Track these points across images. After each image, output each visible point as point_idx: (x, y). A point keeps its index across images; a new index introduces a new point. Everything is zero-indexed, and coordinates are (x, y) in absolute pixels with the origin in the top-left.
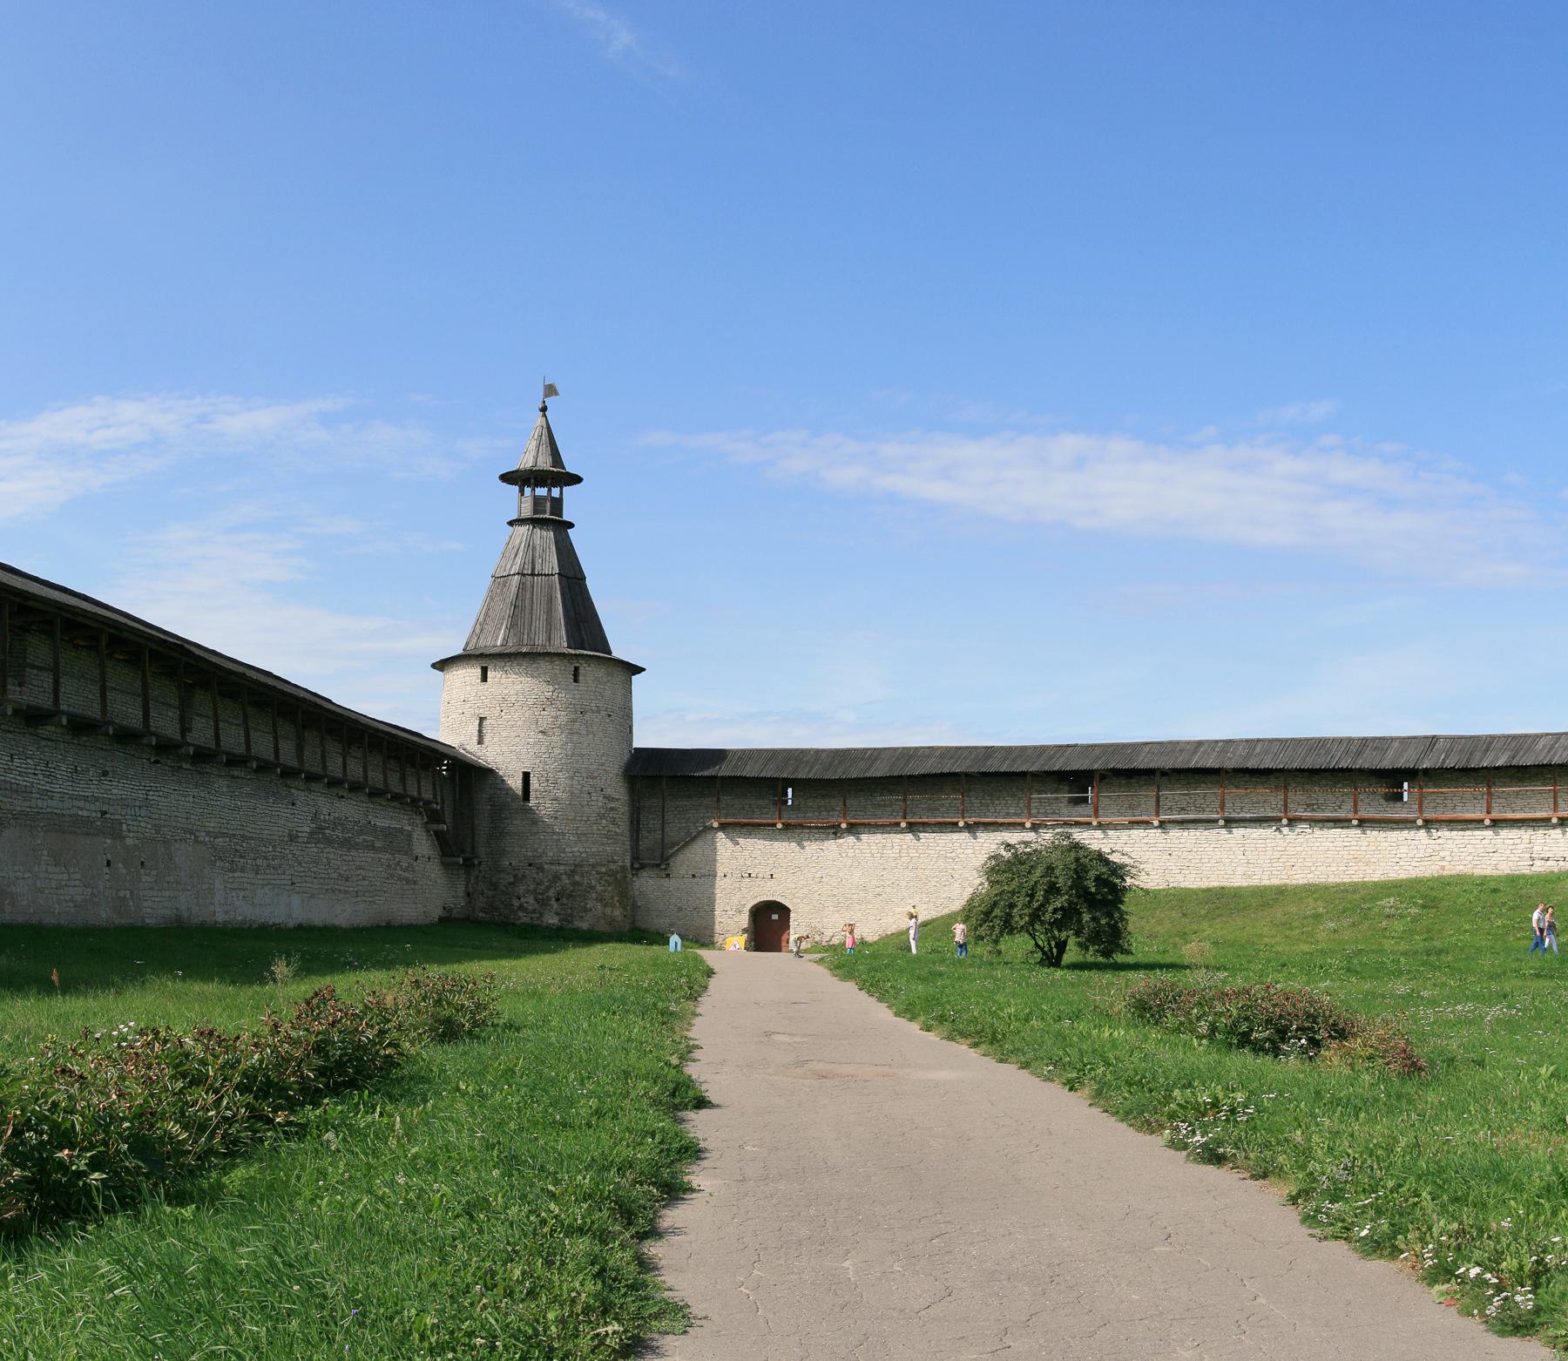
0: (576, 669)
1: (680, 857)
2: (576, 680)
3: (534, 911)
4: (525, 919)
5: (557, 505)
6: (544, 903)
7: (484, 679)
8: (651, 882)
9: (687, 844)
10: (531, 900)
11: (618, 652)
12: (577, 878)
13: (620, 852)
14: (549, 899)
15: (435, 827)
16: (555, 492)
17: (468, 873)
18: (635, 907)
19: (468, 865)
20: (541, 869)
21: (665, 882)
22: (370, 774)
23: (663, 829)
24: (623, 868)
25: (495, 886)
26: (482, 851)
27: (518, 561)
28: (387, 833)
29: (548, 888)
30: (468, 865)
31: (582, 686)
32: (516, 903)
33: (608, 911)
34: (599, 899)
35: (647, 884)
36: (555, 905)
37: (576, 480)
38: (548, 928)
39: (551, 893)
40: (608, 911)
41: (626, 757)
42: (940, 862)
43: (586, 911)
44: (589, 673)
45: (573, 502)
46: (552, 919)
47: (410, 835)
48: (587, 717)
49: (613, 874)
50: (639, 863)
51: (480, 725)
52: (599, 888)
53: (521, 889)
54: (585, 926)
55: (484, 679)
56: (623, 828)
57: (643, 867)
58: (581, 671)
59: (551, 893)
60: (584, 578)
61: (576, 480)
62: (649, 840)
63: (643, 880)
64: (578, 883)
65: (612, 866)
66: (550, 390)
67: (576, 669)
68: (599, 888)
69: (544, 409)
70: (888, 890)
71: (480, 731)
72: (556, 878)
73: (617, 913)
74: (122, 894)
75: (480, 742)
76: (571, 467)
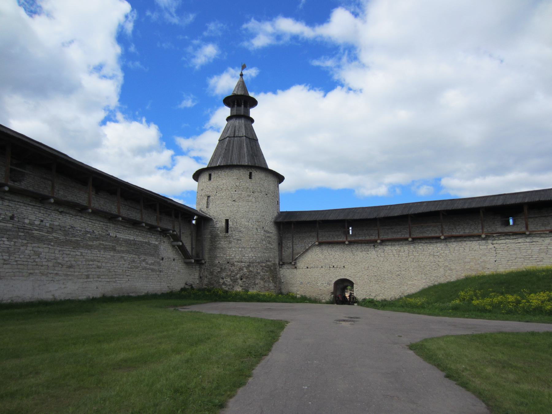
0: (251, 174)
1: (301, 259)
2: (250, 178)
3: (230, 285)
6: (235, 281)
7: (210, 179)
8: (288, 271)
9: (304, 253)
10: (229, 280)
11: (270, 167)
13: (273, 256)
14: (237, 279)
15: (175, 243)
17: (200, 268)
18: (281, 283)
19: (199, 262)
20: (233, 265)
21: (295, 271)
22: (121, 211)
23: (293, 247)
24: (274, 264)
25: (211, 273)
26: (206, 256)
27: (229, 132)
29: (237, 274)
30: (199, 262)
31: (253, 181)
32: (221, 281)
34: (262, 279)
35: (286, 272)
36: (240, 282)
38: (237, 294)
39: (238, 276)
41: (276, 214)
42: (431, 258)
43: (255, 284)
44: (258, 175)
47: (156, 247)
48: (256, 194)
49: (268, 267)
50: (282, 263)
51: (208, 199)
52: (262, 273)
53: (224, 275)
55: (210, 179)
56: (275, 245)
57: (284, 264)
58: (253, 174)
59: (238, 276)
62: (287, 253)
63: (284, 270)
64: (251, 271)
65: (268, 263)
67: (251, 174)
68: (262, 273)
70: (403, 272)
71: (207, 202)
72: (241, 269)
73: (271, 285)
75: (207, 207)
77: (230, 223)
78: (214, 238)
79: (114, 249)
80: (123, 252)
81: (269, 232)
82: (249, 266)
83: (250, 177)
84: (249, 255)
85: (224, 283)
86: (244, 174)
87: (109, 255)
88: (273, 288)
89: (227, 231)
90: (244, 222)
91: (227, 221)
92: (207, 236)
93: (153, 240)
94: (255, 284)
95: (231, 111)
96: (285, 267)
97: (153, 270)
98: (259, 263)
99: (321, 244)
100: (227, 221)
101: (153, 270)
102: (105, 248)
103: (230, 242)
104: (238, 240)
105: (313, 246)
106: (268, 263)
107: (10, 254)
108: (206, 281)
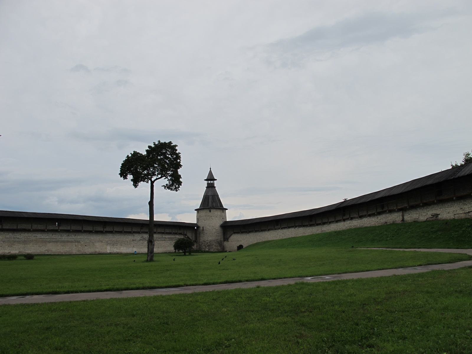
4: (203, 250)
5: (213, 184)
6: (206, 247)
12: (211, 243)
13: (220, 237)
16: (212, 182)
20: (205, 242)
21: (228, 243)
25: (199, 245)
28: (169, 238)
31: (211, 213)
32: (202, 247)
33: (217, 248)
34: (215, 246)
35: (226, 243)
36: (208, 247)
37: (216, 180)
45: (216, 183)
46: (207, 250)
50: (224, 241)
53: (203, 245)
54: (212, 250)
59: (207, 245)
60: (218, 196)
61: (216, 180)
65: (218, 241)
69: (210, 169)
72: (207, 243)
73: (219, 248)
74: (80, 249)
77: (204, 228)
79: (165, 240)
80: (168, 241)
81: (218, 230)
82: (210, 242)
83: (210, 212)
84: (210, 238)
85: (203, 248)
86: (208, 211)
87: (163, 242)
88: (220, 249)
89: (203, 231)
90: (208, 227)
91: (203, 227)
92: (198, 233)
94: (212, 248)
95: (208, 184)
96: (225, 241)
98: (214, 241)
100: (203, 227)
102: (162, 240)
103: (204, 234)
104: (206, 234)
105: (232, 234)
106: (218, 241)
107: (143, 244)
108: (198, 247)
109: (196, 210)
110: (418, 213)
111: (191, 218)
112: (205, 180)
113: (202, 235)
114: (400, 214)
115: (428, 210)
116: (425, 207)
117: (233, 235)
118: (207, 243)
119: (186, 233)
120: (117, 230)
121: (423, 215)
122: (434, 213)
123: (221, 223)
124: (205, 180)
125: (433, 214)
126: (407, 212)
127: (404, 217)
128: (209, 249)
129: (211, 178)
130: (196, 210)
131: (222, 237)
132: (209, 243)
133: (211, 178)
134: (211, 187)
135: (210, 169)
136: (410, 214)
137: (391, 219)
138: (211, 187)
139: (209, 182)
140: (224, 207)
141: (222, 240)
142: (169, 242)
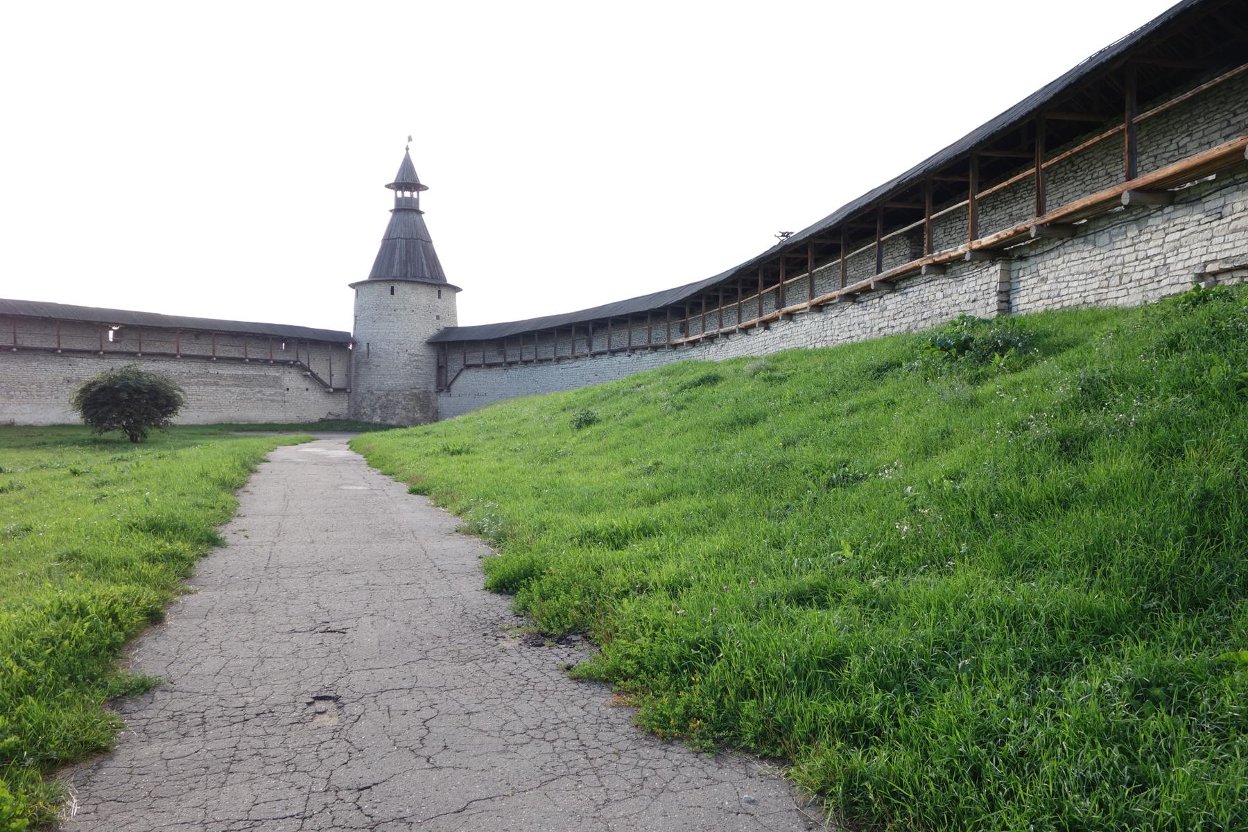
6: (374, 411)
16: (415, 194)
28: (232, 376)
31: (394, 297)
37: (426, 188)
40: (410, 415)
43: (395, 414)
45: (425, 201)
46: (377, 420)
49: (415, 395)
50: (439, 391)
53: (364, 404)
61: (426, 188)
66: (410, 139)
69: (407, 149)
72: (379, 398)
76: (422, 183)
78: (358, 363)
79: (216, 384)
84: (389, 383)
86: (385, 288)
87: (210, 389)
93: (272, 372)
94: (395, 414)
95: (398, 200)
97: (272, 401)
99: (469, 367)
101: (272, 401)
102: (205, 384)
109: (353, 286)
110: (1096, 266)
111: (337, 315)
112: (388, 186)
113: (363, 370)
114: (992, 274)
115: (1177, 235)
116: (1151, 222)
117: (465, 373)
118: (379, 398)
119: (305, 363)
120: (188, 353)
121: (1136, 276)
122: (1225, 260)
123: (431, 331)
124: (388, 186)
125: (1211, 268)
126: (1034, 269)
127: (1009, 302)
128: (384, 419)
129: (407, 181)
130: (353, 286)
131: (434, 379)
132: (384, 399)
133: (407, 181)
134: (407, 212)
135: (407, 149)
136: (1044, 280)
137: (941, 315)
138: (407, 212)
139: (407, 194)
140: (450, 281)
141: (432, 388)
142: (238, 390)
